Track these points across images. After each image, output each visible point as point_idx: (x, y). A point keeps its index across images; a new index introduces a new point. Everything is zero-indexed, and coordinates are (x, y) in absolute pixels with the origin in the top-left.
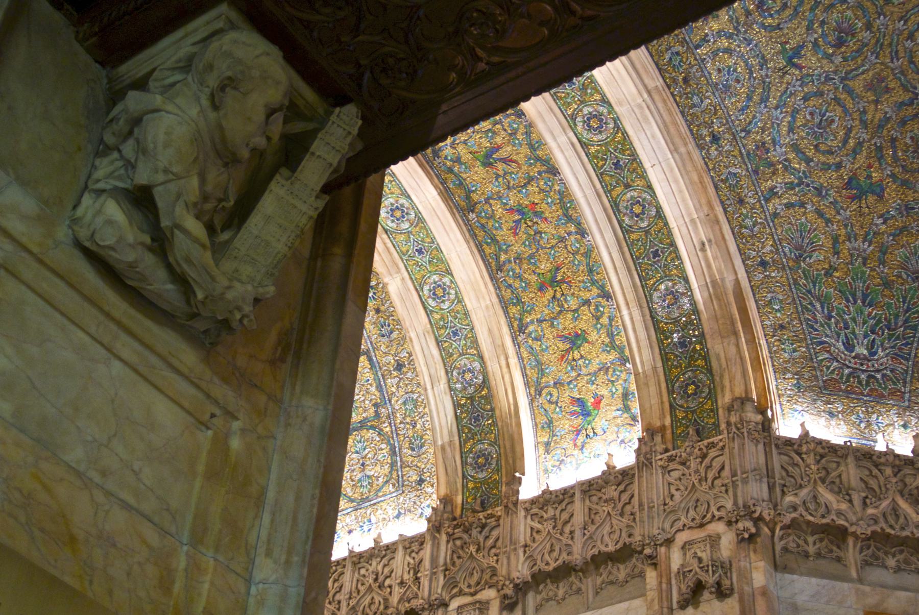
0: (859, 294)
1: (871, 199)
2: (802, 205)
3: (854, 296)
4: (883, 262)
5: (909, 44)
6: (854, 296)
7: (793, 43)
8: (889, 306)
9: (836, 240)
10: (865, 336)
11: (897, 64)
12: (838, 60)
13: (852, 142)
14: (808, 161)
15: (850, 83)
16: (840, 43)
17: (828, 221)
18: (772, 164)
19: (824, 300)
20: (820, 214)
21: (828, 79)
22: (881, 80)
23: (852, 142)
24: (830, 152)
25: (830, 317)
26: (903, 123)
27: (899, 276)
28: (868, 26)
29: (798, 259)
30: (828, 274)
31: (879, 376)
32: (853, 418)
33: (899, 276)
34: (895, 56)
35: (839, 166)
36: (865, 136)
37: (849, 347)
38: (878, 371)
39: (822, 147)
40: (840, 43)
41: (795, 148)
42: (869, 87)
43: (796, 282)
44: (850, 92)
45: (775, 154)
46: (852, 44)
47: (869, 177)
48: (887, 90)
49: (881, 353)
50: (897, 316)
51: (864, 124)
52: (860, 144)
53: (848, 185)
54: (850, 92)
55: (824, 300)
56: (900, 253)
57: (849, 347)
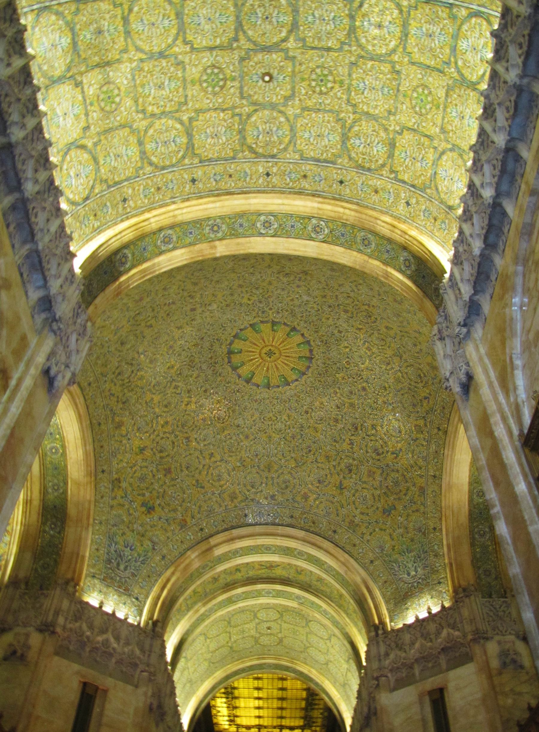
0: (405, 550)
1: (393, 512)
2: (375, 531)
3: (404, 552)
4: (408, 533)
5: (368, 455)
6: (404, 552)
7: (338, 483)
8: (416, 548)
9: (390, 535)
10: (413, 565)
11: (370, 463)
12: (354, 476)
13: (377, 498)
14: (367, 514)
15: (363, 480)
16: (350, 471)
17: (385, 530)
18: (357, 525)
19: (396, 561)
20: (381, 530)
21: (356, 484)
22: (370, 471)
23: (377, 498)
24: (372, 506)
25: (399, 567)
26: (386, 479)
27: (415, 534)
28: (354, 459)
29: (383, 550)
30: (393, 550)
31: (420, 581)
32: (414, 606)
33: (415, 534)
34: (368, 461)
35: (377, 508)
36: (379, 492)
37: (409, 574)
38: (420, 578)
39: (369, 506)
40: (350, 471)
41: (362, 513)
42: (369, 476)
43: (385, 561)
44: (365, 482)
45: (357, 520)
46: (354, 468)
47: (388, 505)
48: (374, 473)
49: (419, 570)
50: (419, 551)
51: (376, 489)
52: (379, 496)
53: (384, 513)
54: (365, 482)
55: (396, 561)
56: (411, 525)
57: (409, 574)
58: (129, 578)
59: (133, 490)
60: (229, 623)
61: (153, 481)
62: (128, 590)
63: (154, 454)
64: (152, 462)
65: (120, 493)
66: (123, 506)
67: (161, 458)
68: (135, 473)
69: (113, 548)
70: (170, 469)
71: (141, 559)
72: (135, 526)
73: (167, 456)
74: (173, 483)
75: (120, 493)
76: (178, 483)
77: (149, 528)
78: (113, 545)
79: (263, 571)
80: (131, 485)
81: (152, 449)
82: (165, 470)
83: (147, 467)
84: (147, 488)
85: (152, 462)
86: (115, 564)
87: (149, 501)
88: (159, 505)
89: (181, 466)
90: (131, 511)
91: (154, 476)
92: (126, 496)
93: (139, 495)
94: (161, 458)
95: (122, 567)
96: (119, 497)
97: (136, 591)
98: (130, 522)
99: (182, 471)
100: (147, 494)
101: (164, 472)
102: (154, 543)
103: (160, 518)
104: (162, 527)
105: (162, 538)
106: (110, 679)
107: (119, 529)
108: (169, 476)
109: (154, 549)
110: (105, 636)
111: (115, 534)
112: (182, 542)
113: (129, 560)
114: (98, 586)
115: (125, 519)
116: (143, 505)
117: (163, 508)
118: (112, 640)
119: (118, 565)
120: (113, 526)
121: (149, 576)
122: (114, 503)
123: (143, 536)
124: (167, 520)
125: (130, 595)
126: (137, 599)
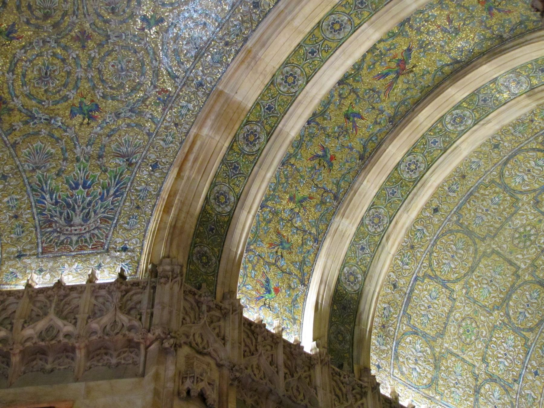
58: (98, 228)
59: (40, 102)
60: (469, 233)
61: (68, 69)
62: (102, 245)
63: (38, 27)
64: (44, 42)
65: (17, 119)
66: (38, 133)
67: (56, 25)
68: (24, 75)
69: (48, 202)
70: (83, 32)
71: (112, 192)
72: (78, 150)
73: (63, 16)
74: (106, 49)
75: (18, 117)
76: (114, 44)
77: (105, 140)
78: (47, 197)
79: (400, 85)
80: (30, 96)
81: (28, 23)
82: (77, 39)
83: (40, 55)
84: (65, 85)
85: (44, 42)
86: (62, 222)
87: (81, 103)
88: (104, 97)
89: (99, 15)
90: (57, 134)
91: (63, 60)
92: (33, 117)
93: (56, 103)
94: (56, 25)
95: (77, 220)
96: (18, 126)
97: (119, 240)
98: (64, 151)
99: (107, 22)
100: (72, 94)
101: (78, 44)
102: (127, 158)
103: (118, 115)
104: (129, 125)
105: (140, 139)
106: (77, 385)
107: (48, 171)
108: (90, 44)
109: (130, 164)
110: (41, 325)
111: (42, 181)
112: (176, 125)
113: (89, 204)
114: (33, 266)
115: (53, 151)
116: (73, 115)
117: (113, 99)
118: (59, 323)
119: (69, 220)
120: (34, 170)
121: (138, 207)
122: (17, 137)
123: (100, 157)
124: (131, 110)
125: (108, 251)
126: (125, 249)
